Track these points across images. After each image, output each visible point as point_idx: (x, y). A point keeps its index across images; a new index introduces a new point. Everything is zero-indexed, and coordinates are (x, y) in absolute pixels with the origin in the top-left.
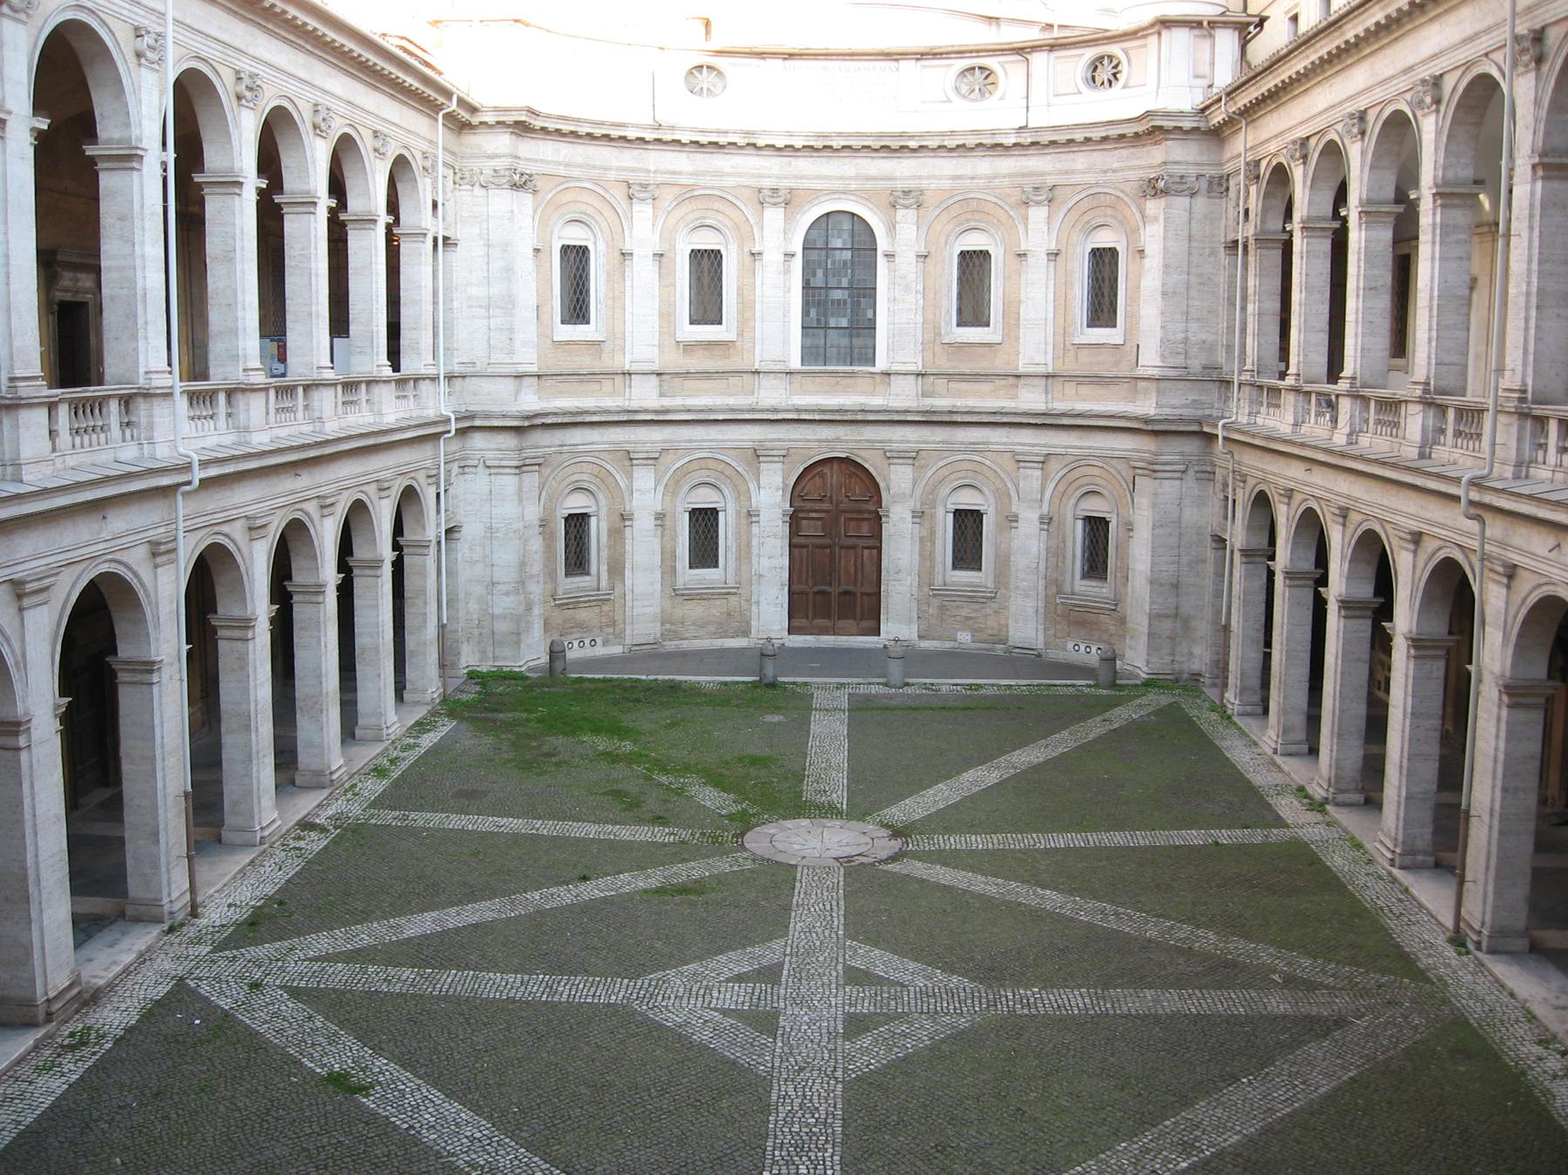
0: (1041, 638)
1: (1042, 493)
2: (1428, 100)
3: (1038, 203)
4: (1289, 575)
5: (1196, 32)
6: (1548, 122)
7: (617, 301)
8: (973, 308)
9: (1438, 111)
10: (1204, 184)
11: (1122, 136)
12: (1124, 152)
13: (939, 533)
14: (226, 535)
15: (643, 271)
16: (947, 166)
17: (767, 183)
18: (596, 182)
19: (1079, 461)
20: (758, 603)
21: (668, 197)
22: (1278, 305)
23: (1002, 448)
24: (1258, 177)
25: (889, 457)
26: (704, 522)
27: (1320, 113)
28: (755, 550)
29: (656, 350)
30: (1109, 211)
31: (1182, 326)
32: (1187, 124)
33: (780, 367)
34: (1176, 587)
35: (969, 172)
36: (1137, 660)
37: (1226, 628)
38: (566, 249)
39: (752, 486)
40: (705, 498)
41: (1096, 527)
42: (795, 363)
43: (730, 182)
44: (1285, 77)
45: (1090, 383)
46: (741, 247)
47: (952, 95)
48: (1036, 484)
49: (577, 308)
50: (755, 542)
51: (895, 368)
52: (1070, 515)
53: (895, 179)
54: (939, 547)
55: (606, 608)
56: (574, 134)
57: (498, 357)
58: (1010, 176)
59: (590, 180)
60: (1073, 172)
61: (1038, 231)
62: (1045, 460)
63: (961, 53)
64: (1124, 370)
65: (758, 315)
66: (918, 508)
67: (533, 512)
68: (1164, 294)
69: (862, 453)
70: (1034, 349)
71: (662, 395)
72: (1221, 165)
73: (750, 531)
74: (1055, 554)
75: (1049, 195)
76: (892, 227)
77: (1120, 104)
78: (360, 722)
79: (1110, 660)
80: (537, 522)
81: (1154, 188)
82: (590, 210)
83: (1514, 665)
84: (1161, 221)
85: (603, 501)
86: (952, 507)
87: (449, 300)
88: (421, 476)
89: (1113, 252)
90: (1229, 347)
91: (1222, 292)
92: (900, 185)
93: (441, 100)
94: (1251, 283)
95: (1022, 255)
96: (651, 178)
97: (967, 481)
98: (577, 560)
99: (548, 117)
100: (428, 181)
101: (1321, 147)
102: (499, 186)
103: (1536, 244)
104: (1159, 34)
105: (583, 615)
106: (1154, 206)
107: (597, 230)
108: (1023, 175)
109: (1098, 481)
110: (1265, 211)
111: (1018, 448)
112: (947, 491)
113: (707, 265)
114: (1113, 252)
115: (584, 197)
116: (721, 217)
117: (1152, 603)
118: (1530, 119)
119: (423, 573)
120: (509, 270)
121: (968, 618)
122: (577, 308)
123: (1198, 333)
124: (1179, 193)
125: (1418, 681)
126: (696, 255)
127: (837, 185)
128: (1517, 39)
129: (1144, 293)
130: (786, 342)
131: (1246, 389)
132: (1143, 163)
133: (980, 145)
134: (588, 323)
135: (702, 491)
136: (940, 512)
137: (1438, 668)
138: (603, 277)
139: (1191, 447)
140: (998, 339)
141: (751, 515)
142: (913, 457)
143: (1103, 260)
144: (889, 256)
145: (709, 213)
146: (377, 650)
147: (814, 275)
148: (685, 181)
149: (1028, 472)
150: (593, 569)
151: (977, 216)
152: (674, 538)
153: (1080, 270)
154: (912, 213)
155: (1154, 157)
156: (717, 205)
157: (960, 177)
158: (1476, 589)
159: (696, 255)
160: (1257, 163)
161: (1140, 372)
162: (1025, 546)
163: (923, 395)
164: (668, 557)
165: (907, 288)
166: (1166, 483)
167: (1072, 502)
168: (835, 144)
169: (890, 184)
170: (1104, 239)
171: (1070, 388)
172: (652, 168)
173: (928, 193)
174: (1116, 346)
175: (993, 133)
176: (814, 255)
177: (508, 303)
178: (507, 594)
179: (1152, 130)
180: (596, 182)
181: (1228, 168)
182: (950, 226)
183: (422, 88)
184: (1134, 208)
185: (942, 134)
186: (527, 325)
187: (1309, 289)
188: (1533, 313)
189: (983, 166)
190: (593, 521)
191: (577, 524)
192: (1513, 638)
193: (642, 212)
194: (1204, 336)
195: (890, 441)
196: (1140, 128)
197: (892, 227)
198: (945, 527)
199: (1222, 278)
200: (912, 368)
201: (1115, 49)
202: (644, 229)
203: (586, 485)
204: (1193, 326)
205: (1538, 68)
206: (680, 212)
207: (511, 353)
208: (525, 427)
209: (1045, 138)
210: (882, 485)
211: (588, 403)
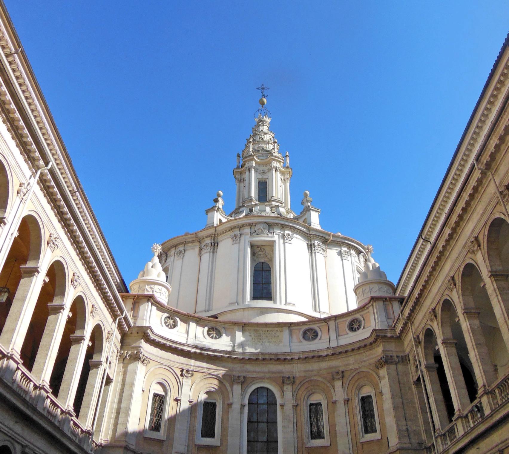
3: (338, 379)
9: (480, 249)
11: (365, 346)
12: (367, 353)
24: (420, 343)
27: (437, 293)
30: (365, 379)
32: (389, 335)
38: (155, 395)
44: (421, 287)
58: (326, 369)
75: (342, 375)
76: (283, 392)
84: (387, 376)
89: (370, 397)
96: (191, 369)
99: (156, 335)
101: (441, 307)
106: (383, 372)
110: (426, 355)
114: (370, 397)
124: (391, 363)
132: (375, 356)
133: (313, 357)
153: (357, 406)
155: (379, 351)
160: (418, 337)
168: (260, 358)
172: (193, 364)
175: (318, 351)
184: (375, 375)
189: (315, 366)
193: (187, 382)
196: (372, 340)
197: (283, 392)
206: (202, 384)
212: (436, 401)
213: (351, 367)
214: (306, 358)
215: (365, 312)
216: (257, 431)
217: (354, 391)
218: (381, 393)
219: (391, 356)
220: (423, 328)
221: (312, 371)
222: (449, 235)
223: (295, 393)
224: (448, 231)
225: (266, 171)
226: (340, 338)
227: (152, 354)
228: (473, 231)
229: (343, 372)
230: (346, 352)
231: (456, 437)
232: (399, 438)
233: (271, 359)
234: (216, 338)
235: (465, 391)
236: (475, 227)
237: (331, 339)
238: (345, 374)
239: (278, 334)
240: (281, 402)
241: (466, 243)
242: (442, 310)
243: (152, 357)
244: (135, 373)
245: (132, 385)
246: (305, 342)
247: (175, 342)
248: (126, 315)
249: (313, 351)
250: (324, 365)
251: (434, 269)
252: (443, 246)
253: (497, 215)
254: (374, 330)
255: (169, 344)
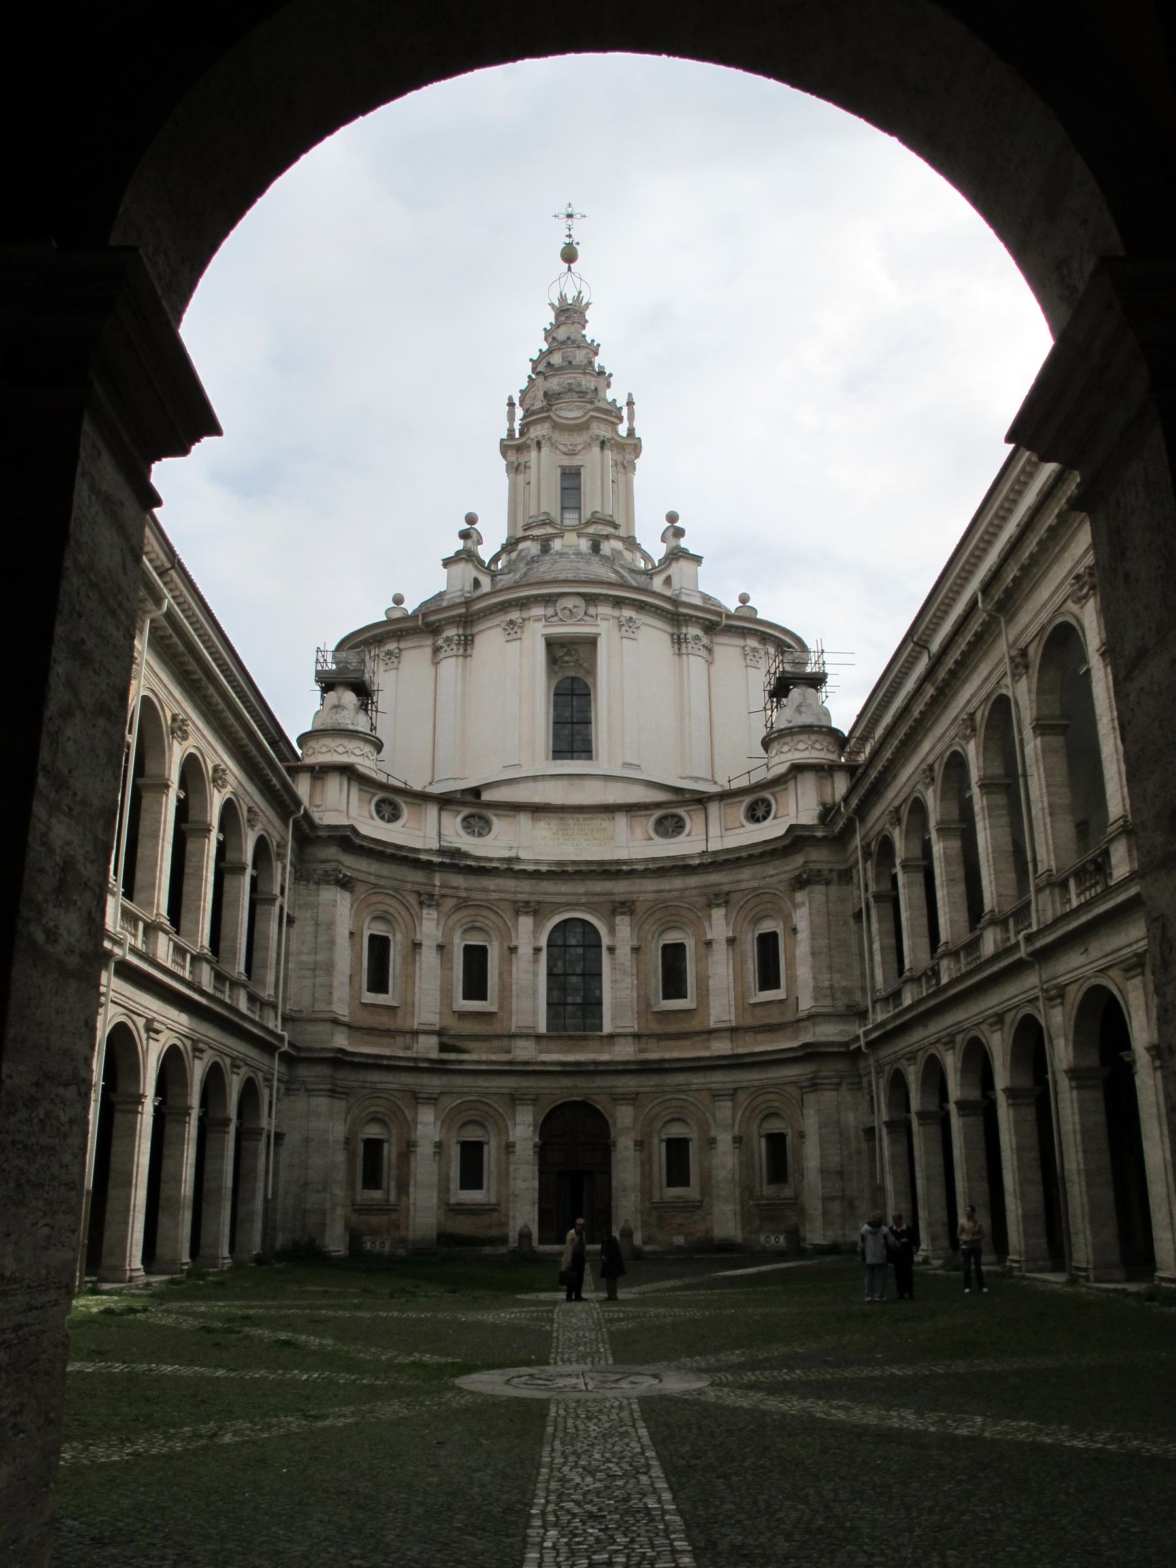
0: (739, 1233)
1: (734, 1121)
2: (968, 732)
3: (718, 906)
4: (921, 1115)
5: (821, 774)
6: (1038, 701)
7: (409, 978)
8: (674, 984)
10: (835, 875)
11: (774, 850)
12: (777, 863)
13: (656, 1158)
14: (134, 1022)
15: (429, 957)
16: (651, 885)
17: (521, 897)
18: (396, 890)
19: (760, 1090)
20: (514, 1217)
21: (449, 903)
22: (893, 941)
23: (701, 1087)
25: (618, 1099)
26: (472, 1154)
27: (905, 784)
28: (512, 1175)
29: (438, 1016)
30: (769, 906)
31: (827, 976)
32: (819, 834)
33: (530, 1031)
34: (840, 1174)
35: (667, 887)
36: (816, 1235)
37: (881, 1188)
38: (372, 938)
39: (509, 1123)
40: (473, 1134)
41: (776, 1142)
42: (542, 1028)
43: (494, 896)
44: (880, 767)
45: (764, 1032)
46: (501, 944)
47: (653, 835)
48: (729, 1113)
49: (379, 982)
50: (512, 1168)
51: (619, 1030)
52: (755, 1134)
53: (612, 894)
54: (656, 1168)
55: (393, 1216)
56: (382, 853)
57: (320, 1006)
58: (696, 888)
59: (392, 889)
60: (743, 881)
61: (719, 926)
62: (733, 1094)
63: (658, 805)
64: (789, 1017)
65: (514, 993)
66: (639, 1138)
67: (338, 1130)
68: (813, 954)
69: (595, 1097)
70: (721, 1009)
71: (443, 1048)
72: (846, 861)
73: (508, 1163)
74: (746, 1165)
76: (612, 930)
77: (772, 829)
78: (202, 1252)
79: (794, 1235)
80: (342, 1139)
81: (800, 882)
82: (391, 910)
83: (1074, 1057)
84: (807, 904)
85: (394, 1131)
86: (664, 1137)
87: (287, 962)
88: (260, 1075)
89: (773, 936)
90: (863, 989)
91: (855, 950)
92: (617, 898)
93: (293, 808)
94: (875, 926)
95: (709, 944)
96: (437, 891)
97: (675, 1116)
98: (372, 1178)
100: (279, 865)
102: (327, 883)
103: (1043, 776)
104: (795, 778)
105: (375, 1220)
107: (396, 926)
108: (706, 887)
109: (776, 1104)
111: (713, 1086)
112: (661, 1124)
113: (476, 958)
114: (773, 936)
115: (388, 900)
116: (487, 922)
117: (823, 1187)
118: (1027, 702)
119: (255, 1156)
120: (332, 942)
121: (681, 1225)
122: (379, 982)
123: (840, 982)
124: (817, 883)
125: (1018, 1126)
126: (468, 949)
127: (573, 899)
128: (1012, 659)
129: (798, 960)
130: (535, 1013)
131: (878, 1006)
133: (673, 867)
134: (386, 992)
135: (470, 1128)
136: (656, 1141)
137: (1030, 1113)
138: (399, 960)
139: (841, 1066)
140: (694, 1006)
141: (509, 1147)
142: (633, 1099)
143: (768, 945)
144: (611, 950)
145: (480, 918)
146: (220, 1189)
147: (556, 965)
148: (463, 894)
149: (722, 1103)
150: (385, 1185)
151: (673, 918)
152: (448, 1164)
154: (627, 919)
156: (485, 912)
157: (661, 891)
158: (1043, 1024)
159: (468, 949)
160: (869, 845)
161: (801, 1014)
162: (725, 1161)
163: (641, 1051)
164: (444, 1180)
165: (625, 972)
166: (826, 1093)
167: (757, 1122)
168: (569, 869)
169: (611, 898)
170: (767, 926)
171: (749, 1037)
172: (437, 883)
173: (638, 904)
174: (781, 1001)
175: (683, 857)
176: (555, 950)
177: (329, 967)
178: (317, 1192)
179: (797, 839)
180: (396, 890)
181: (852, 859)
182: (655, 927)
183: (282, 792)
185: (646, 860)
186: (344, 991)
187: (911, 906)
188: (1048, 819)
189: (678, 883)
190: (386, 1146)
191: (373, 1147)
192: (1071, 1038)
194: (844, 984)
195: (616, 1087)
196: (786, 842)
197: (612, 930)
198: (660, 1152)
199: (853, 940)
200: (631, 1030)
201: (767, 795)
202: (430, 927)
203: (380, 1116)
204: (836, 977)
205: (1027, 672)
206: (456, 917)
207: (330, 1003)
208: (340, 1060)
209: (722, 858)
210: (610, 1121)
211: (387, 1052)
212: (882, 948)
213: (744, 886)
214: (659, 869)
215: (779, 788)
216: (564, 989)
217: (745, 926)
218: (795, 930)
219: (819, 871)
220: (879, 833)
221: (670, 891)
222: (932, 696)
223: (637, 927)
224: (930, 691)
225: (579, 447)
226: (729, 832)
227: (359, 871)
228: (969, 701)
229: (728, 893)
230: (739, 859)
231: (901, 1004)
232: (815, 999)
233: (591, 871)
234: (480, 835)
235: (925, 941)
236: (973, 696)
237: (711, 834)
238: (734, 898)
239: (606, 824)
240: (609, 943)
241: (956, 718)
242: (910, 813)
243: (361, 876)
244: (335, 906)
245: (331, 925)
246: (658, 840)
247: (401, 848)
248: (305, 810)
249: (674, 858)
250: (693, 881)
251: (904, 744)
252: (921, 712)
253: (1004, 691)
254: (792, 828)
255: (390, 851)
